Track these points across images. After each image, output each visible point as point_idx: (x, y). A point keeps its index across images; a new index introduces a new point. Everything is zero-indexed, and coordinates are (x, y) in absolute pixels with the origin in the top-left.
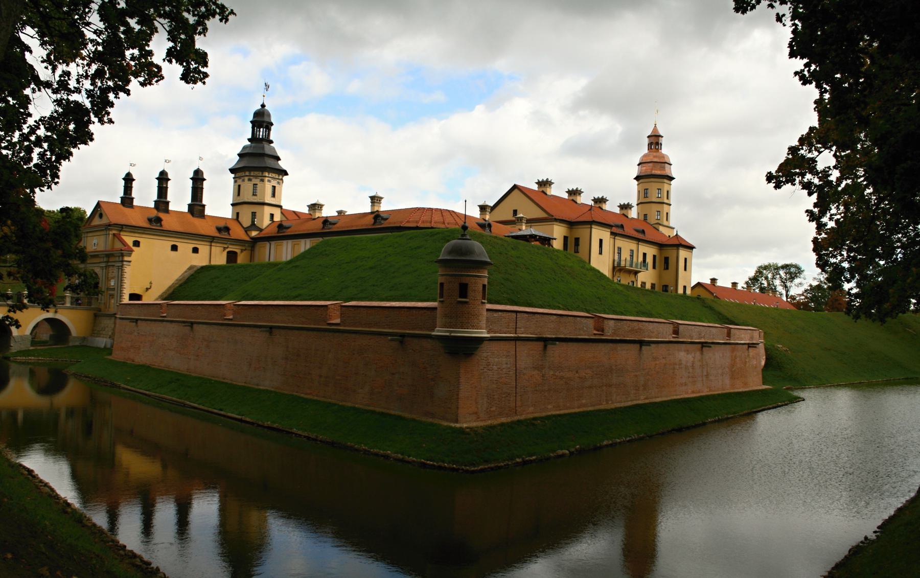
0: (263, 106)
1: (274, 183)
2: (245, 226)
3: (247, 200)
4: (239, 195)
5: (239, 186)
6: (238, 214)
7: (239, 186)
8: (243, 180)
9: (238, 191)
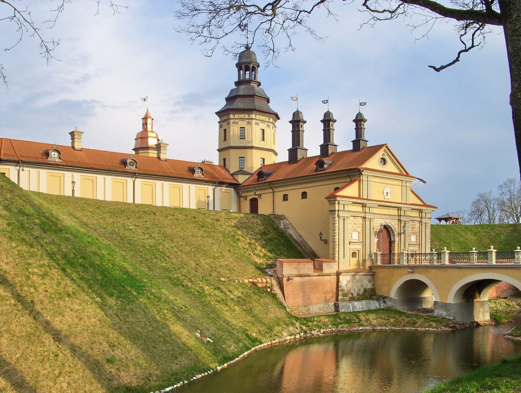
0: (247, 48)
1: (263, 126)
2: (231, 172)
3: (232, 144)
4: (225, 140)
5: (225, 130)
6: (225, 159)
7: (225, 130)
8: (228, 124)
9: (224, 135)
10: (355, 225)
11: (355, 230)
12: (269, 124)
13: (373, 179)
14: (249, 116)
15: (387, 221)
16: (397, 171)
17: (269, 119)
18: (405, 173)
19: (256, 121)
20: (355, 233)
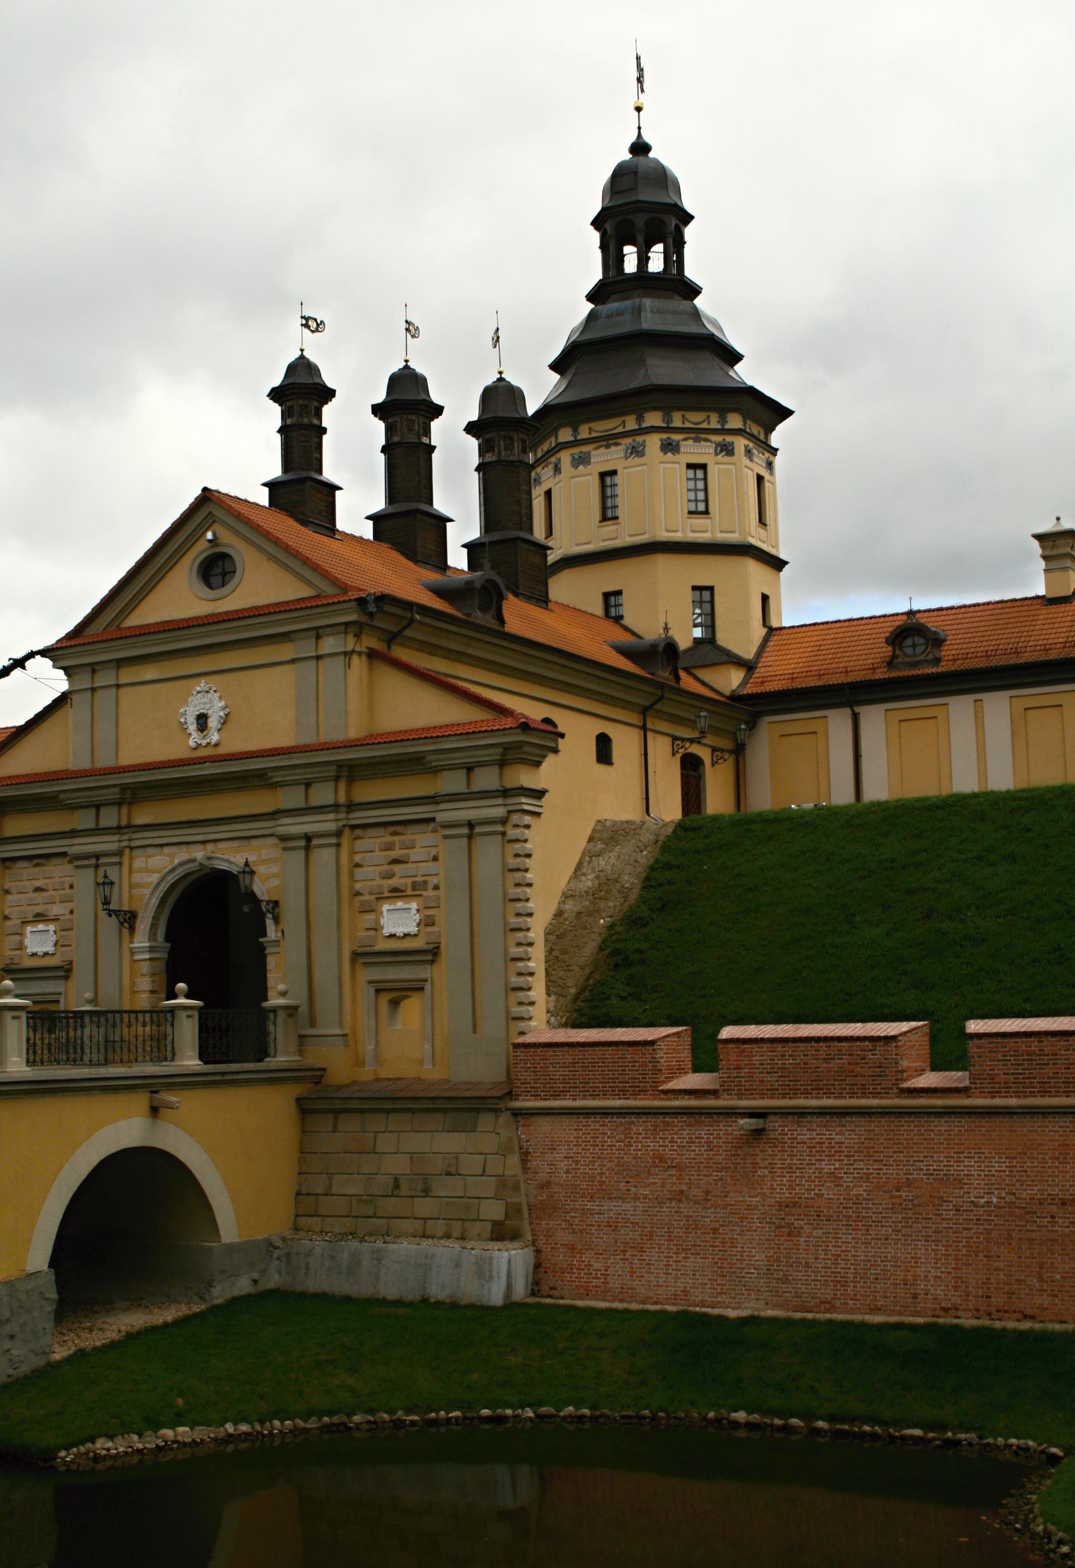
0: (640, 148)
10: (39, 897)
11: (40, 917)
12: (639, 439)
13: (127, 675)
15: (199, 854)
16: (306, 592)
17: (640, 419)
18: (329, 590)
19: (576, 451)
20: (41, 927)
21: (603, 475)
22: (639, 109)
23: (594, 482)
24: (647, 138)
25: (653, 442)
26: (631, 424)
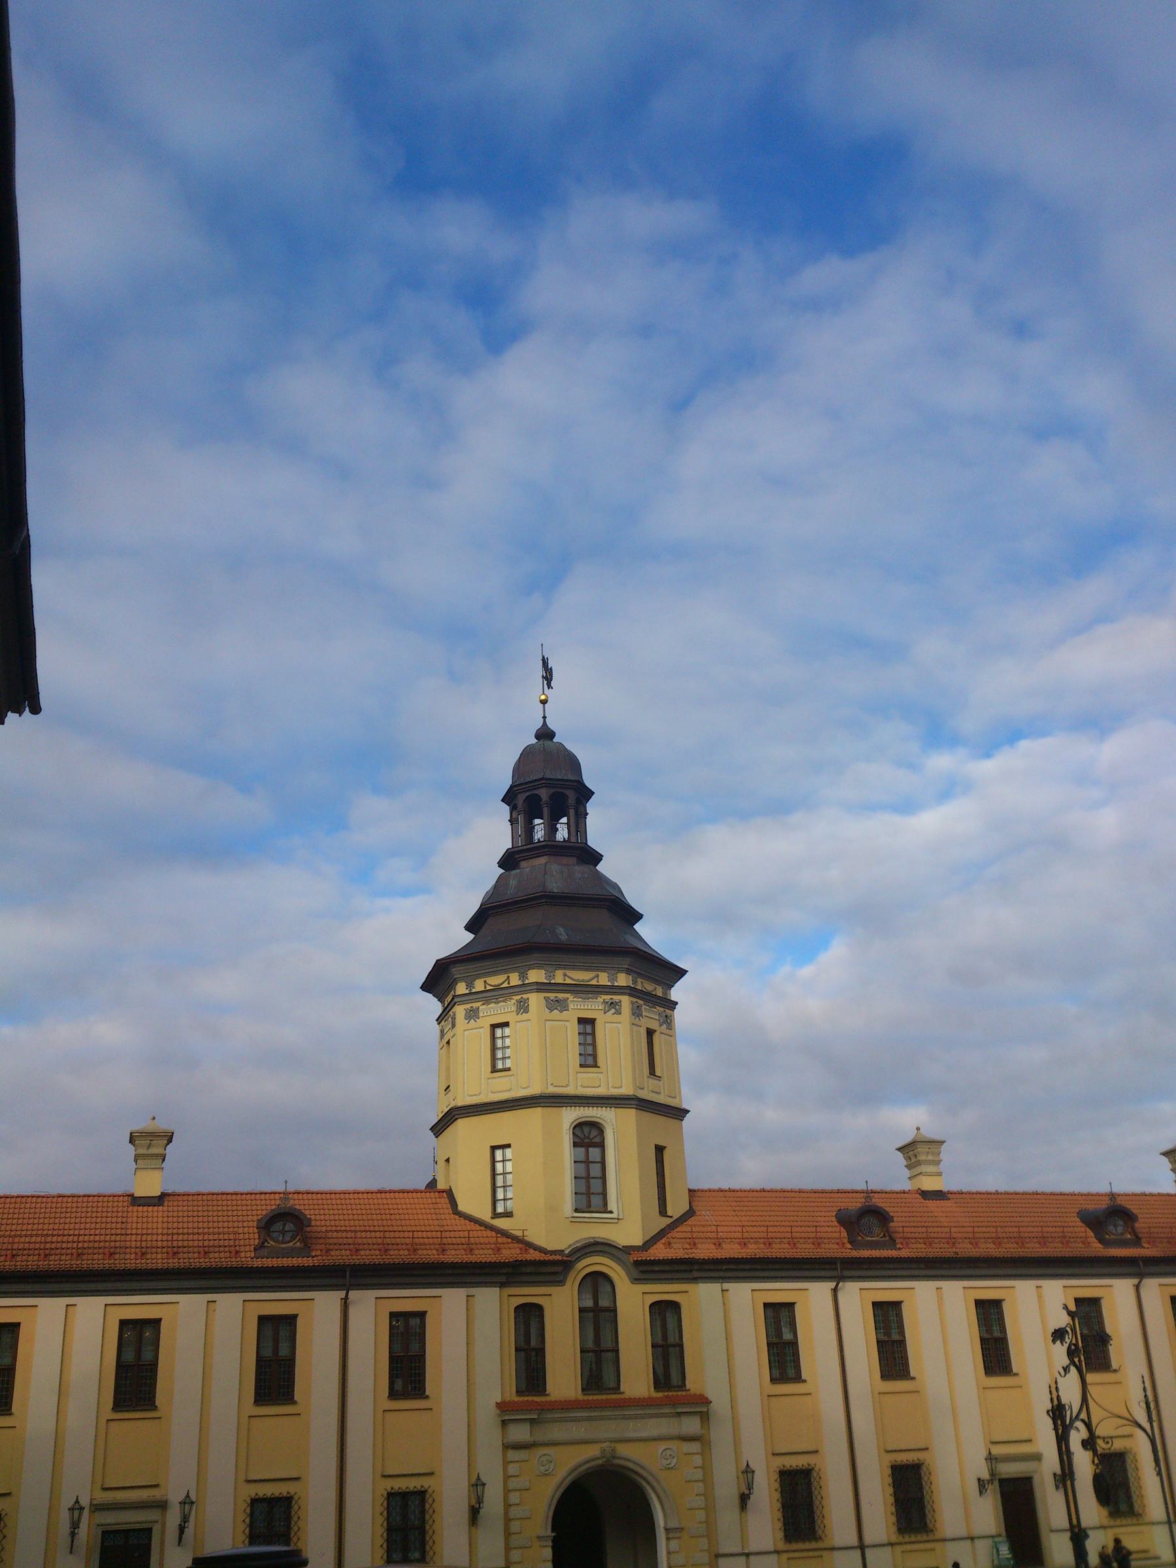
0: (545, 734)
12: (616, 998)
14: (523, 976)
21: (581, 1021)
22: (544, 702)
23: (573, 1028)
24: (551, 725)
25: (626, 1001)
26: (603, 979)
